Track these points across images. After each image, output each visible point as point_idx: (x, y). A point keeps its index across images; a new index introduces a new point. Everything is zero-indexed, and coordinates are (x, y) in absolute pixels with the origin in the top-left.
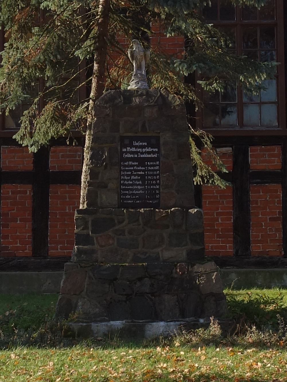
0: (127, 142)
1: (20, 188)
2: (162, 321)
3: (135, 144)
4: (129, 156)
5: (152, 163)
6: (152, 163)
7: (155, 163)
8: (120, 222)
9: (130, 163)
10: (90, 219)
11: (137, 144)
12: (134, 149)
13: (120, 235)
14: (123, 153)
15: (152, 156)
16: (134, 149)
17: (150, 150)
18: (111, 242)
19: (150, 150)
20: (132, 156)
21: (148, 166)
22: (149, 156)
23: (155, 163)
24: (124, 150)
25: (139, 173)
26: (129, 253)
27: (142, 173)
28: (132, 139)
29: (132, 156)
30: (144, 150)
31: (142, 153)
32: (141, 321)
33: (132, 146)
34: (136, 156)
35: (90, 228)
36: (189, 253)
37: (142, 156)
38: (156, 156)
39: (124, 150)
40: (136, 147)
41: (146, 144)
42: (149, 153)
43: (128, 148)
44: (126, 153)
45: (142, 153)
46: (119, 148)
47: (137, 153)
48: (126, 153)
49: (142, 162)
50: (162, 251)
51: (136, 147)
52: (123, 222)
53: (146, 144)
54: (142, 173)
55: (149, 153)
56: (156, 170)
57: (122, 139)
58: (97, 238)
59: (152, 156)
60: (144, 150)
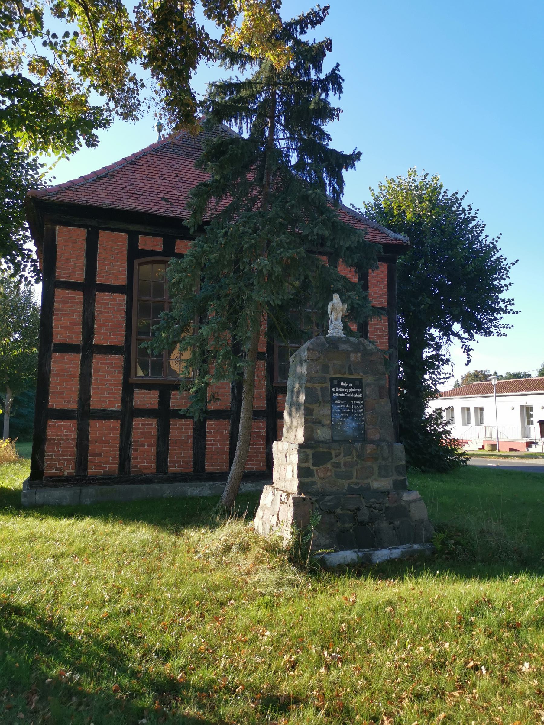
0: (335, 382)
1: (147, 421)
2: (383, 548)
3: (342, 384)
4: (338, 395)
5: (357, 402)
6: (357, 402)
7: (359, 402)
8: (337, 456)
9: (339, 401)
11: (344, 385)
12: (341, 389)
13: (337, 467)
14: (332, 392)
15: (357, 395)
16: (341, 389)
17: (354, 390)
18: (329, 474)
19: (354, 390)
20: (340, 395)
21: (354, 404)
22: (354, 396)
23: (359, 402)
24: (334, 390)
25: (347, 411)
26: (345, 483)
27: (349, 411)
28: (340, 380)
29: (340, 395)
30: (350, 390)
31: (349, 393)
32: (366, 550)
33: (340, 386)
34: (343, 395)
36: (395, 483)
37: (349, 395)
38: (360, 395)
39: (334, 390)
40: (343, 387)
41: (351, 385)
42: (354, 393)
43: (337, 388)
44: (336, 392)
45: (349, 393)
46: (329, 388)
47: (344, 392)
48: (336, 392)
49: (349, 401)
50: (372, 481)
51: (343, 387)
52: (339, 456)
53: (351, 385)
54: (349, 411)
55: (354, 393)
56: (361, 409)
57: (332, 379)
58: (317, 471)
59: (357, 395)
60: (350, 390)
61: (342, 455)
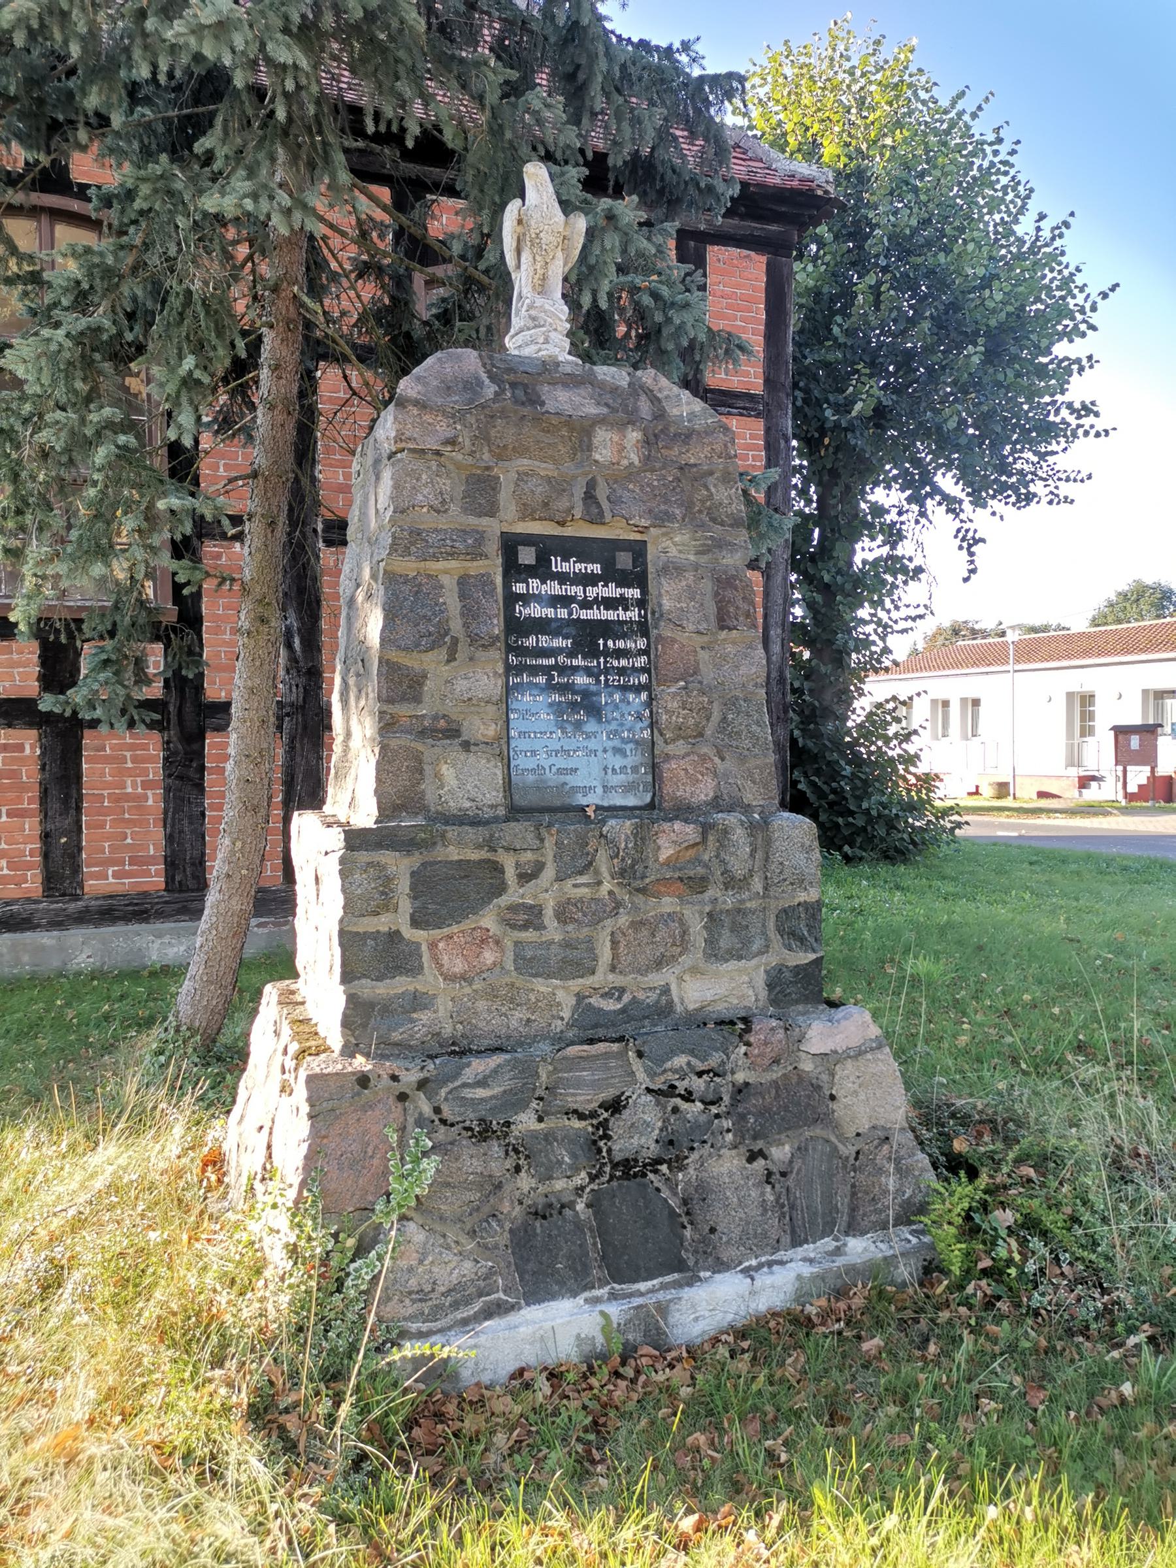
3: (559, 565)
5: (621, 644)
7: (630, 645)
8: (525, 877)
10: (400, 866)
11: (565, 567)
13: (525, 927)
15: (621, 614)
16: (553, 588)
17: (611, 591)
18: (489, 957)
21: (607, 653)
22: (610, 615)
23: (630, 645)
24: (520, 588)
28: (547, 548)
30: (592, 592)
31: (586, 604)
35: (406, 906)
37: (585, 615)
38: (634, 614)
39: (520, 588)
40: (563, 578)
41: (596, 568)
42: (610, 604)
43: (534, 583)
45: (586, 604)
46: (499, 580)
47: (564, 601)
51: (563, 578)
53: (596, 568)
55: (610, 604)
57: (510, 545)
58: (433, 945)
59: (621, 614)
60: (592, 592)
61: (549, 873)
